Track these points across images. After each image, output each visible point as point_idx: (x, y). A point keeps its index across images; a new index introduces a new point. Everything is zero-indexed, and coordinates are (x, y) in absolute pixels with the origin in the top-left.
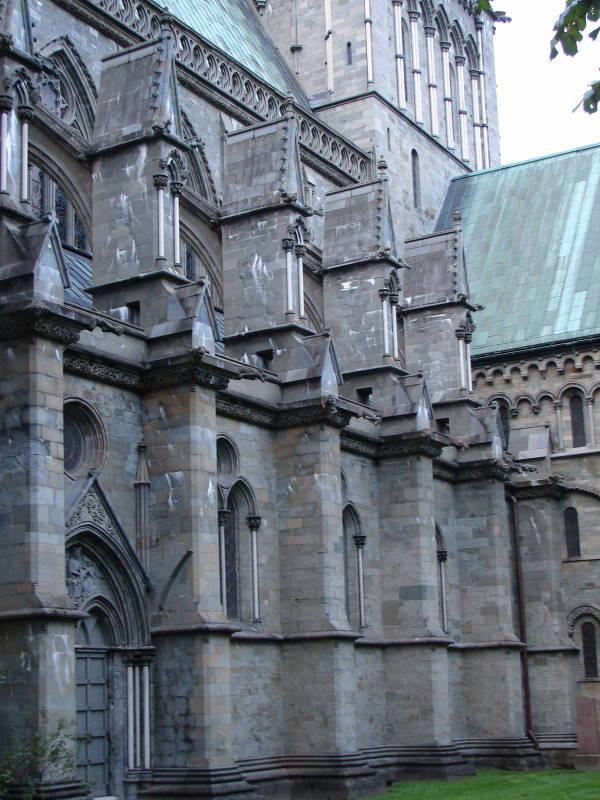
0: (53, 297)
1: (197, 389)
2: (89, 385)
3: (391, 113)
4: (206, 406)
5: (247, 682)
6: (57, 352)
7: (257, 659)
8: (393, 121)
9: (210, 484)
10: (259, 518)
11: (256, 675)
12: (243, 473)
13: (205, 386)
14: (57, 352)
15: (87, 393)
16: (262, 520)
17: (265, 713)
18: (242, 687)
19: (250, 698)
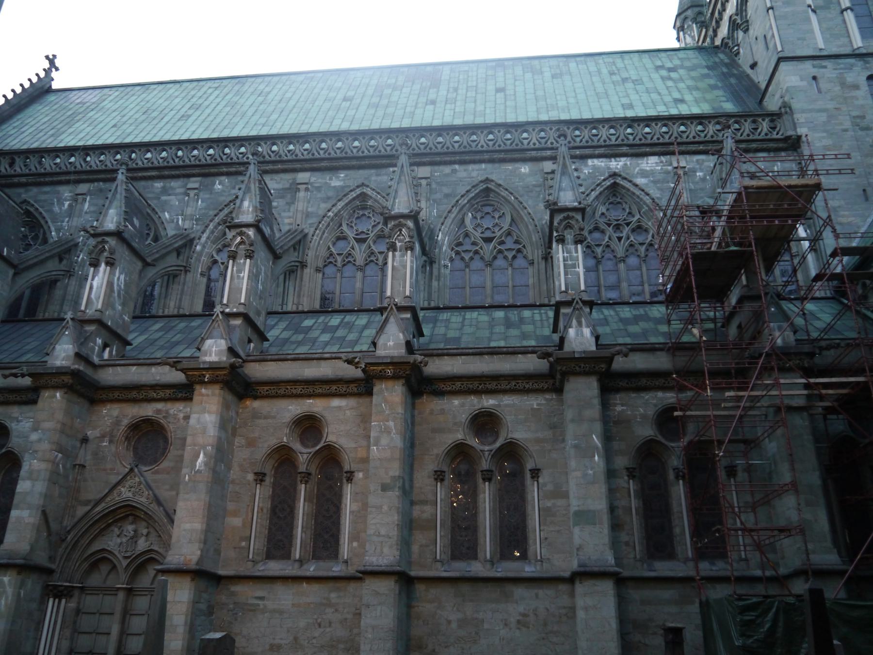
0: (64, 362)
1: (197, 387)
2: (160, 406)
3: (816, 62)
4: (205, 398)
5: (315, 617)
6: (58, 395)
7: (333, 595)
8: (825, 67)
9: (202, 455)
10: (353, 472)
11: (329, 610)
12: (332, 438)
13: (202, 383)
14: (58, 395)
15: (158, 411)
16: (356, 474)
17: (342, 646)
18: (311, 621)
19: (322, 630)
